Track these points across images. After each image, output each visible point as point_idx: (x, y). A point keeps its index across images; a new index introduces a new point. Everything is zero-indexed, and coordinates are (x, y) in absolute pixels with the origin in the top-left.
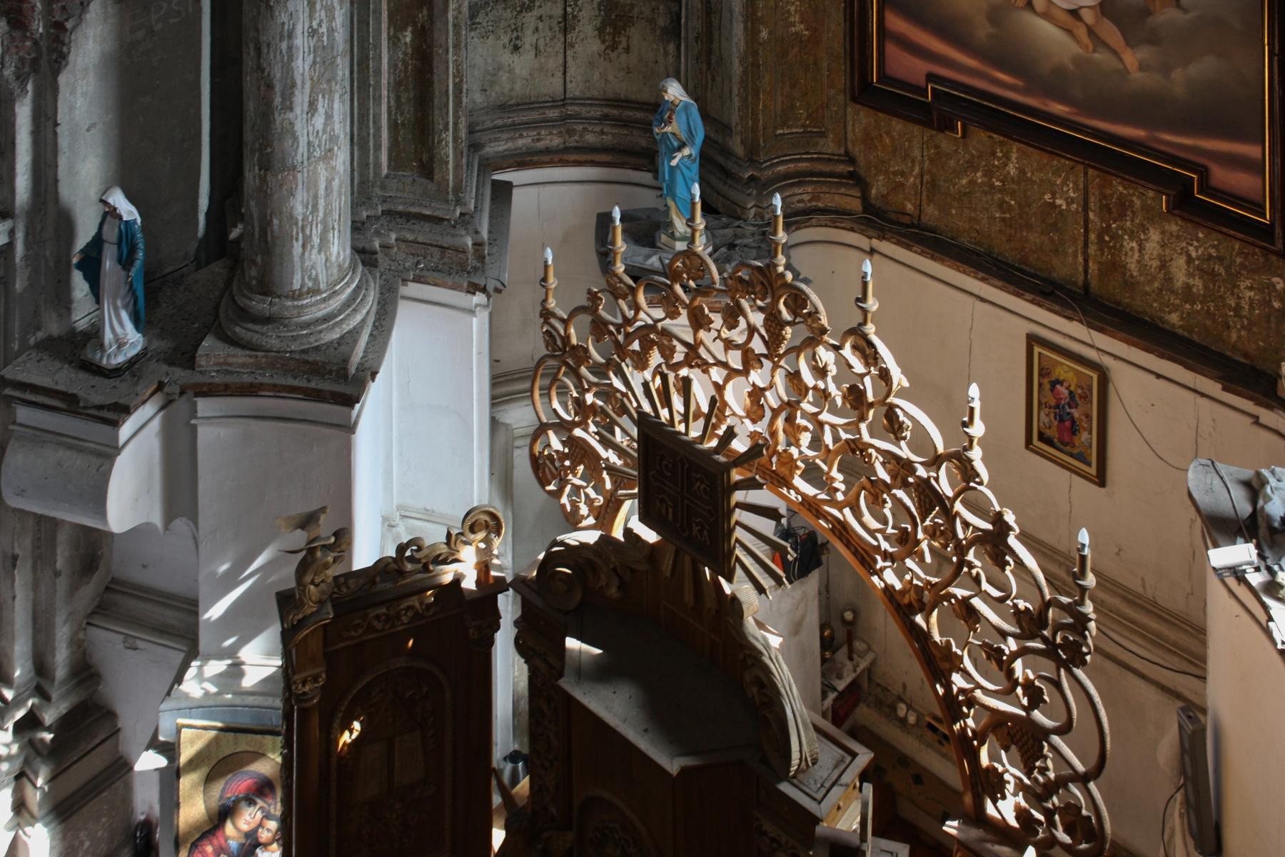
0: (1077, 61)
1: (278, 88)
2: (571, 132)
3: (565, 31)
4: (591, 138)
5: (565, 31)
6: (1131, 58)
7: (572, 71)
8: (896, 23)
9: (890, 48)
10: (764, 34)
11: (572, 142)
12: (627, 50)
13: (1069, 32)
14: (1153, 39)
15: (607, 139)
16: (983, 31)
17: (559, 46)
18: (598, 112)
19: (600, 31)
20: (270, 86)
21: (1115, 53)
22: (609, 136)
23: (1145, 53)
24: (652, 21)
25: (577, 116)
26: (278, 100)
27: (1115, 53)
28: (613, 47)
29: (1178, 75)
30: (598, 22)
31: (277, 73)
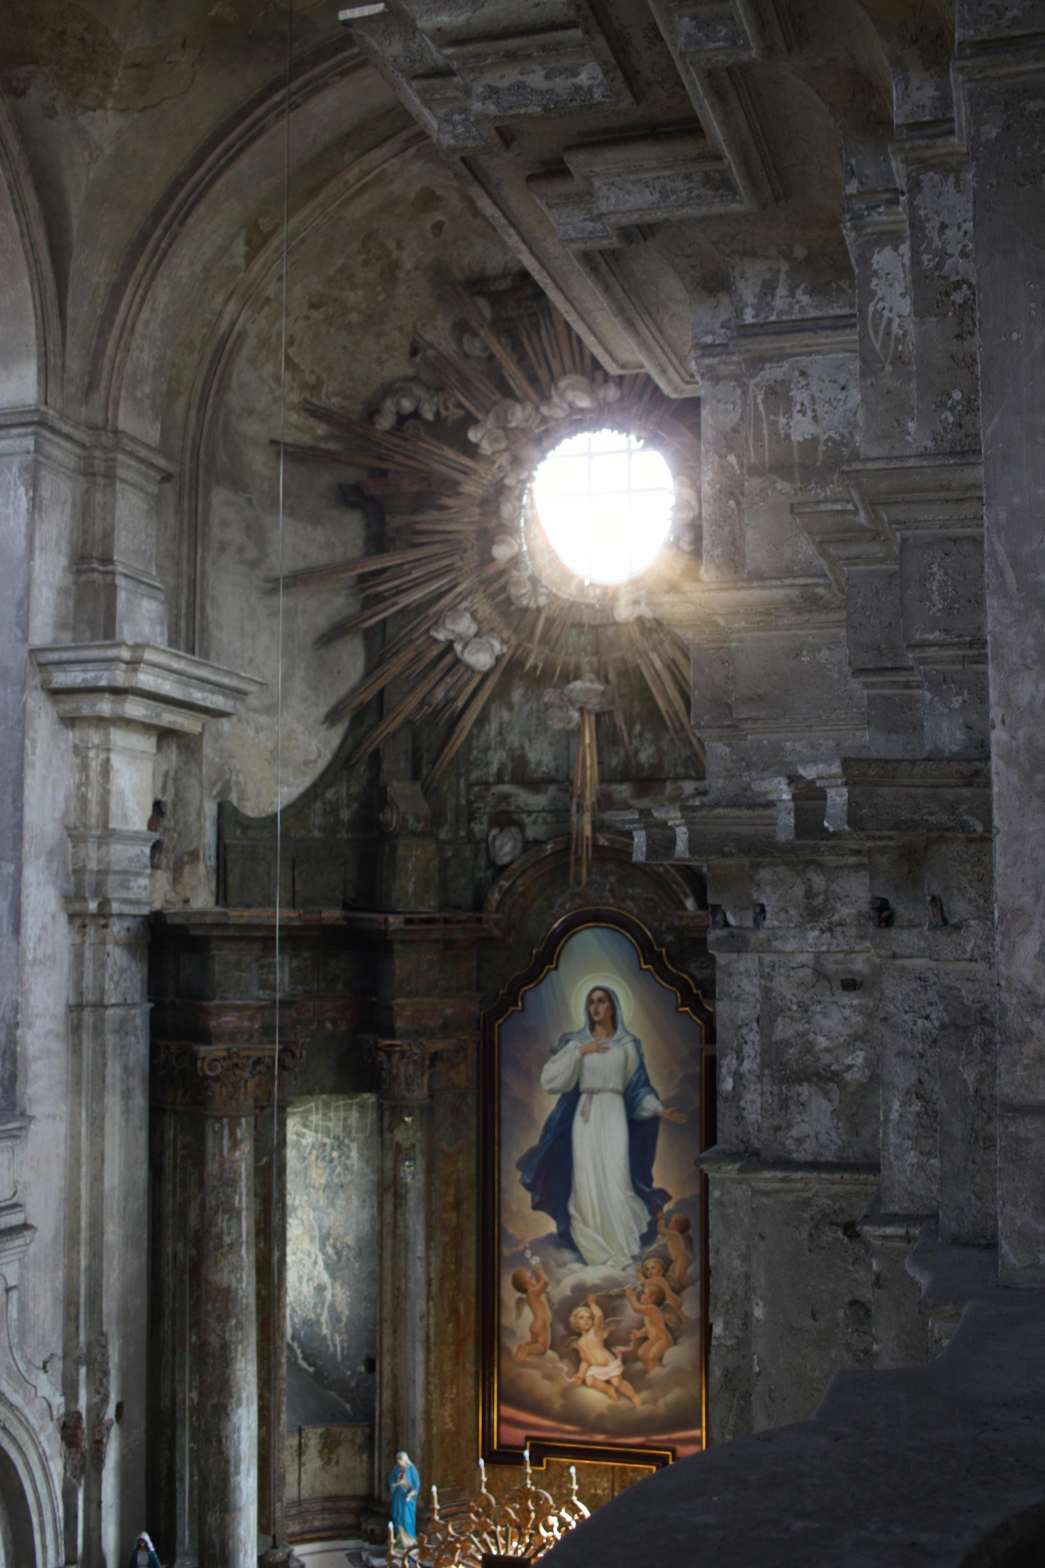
0: (610, 1408)
1: (232, 1462)
2: (305, 1521)
3: (300, 1456)
4: (317, 1524)
5: (300, 1456)
6: (637, 1399)
7: (304, 1481)
8: (508, 1411)
9: (503, 1427)
10: (435, 1430)
11: (306, 1527)
12: (337, 1463)
13: (605, 1392)
14: (649, 1386)
15: (327, 1523)
16: (558, 1403)
17: (296, 1466)
18: (318, 1508)
19: (321, 1452)
20: (227, 1462)
21: (629, 1399)
22: (329, 1520)
23: (645, 1395)
24: (353, 1442)
25: (307, 1511)
26: (232, 1469)
27: (629, 1399)
28: (328, 1463)
29: (661, 1403)
30: (319, 1447)
31: (232, 1453)
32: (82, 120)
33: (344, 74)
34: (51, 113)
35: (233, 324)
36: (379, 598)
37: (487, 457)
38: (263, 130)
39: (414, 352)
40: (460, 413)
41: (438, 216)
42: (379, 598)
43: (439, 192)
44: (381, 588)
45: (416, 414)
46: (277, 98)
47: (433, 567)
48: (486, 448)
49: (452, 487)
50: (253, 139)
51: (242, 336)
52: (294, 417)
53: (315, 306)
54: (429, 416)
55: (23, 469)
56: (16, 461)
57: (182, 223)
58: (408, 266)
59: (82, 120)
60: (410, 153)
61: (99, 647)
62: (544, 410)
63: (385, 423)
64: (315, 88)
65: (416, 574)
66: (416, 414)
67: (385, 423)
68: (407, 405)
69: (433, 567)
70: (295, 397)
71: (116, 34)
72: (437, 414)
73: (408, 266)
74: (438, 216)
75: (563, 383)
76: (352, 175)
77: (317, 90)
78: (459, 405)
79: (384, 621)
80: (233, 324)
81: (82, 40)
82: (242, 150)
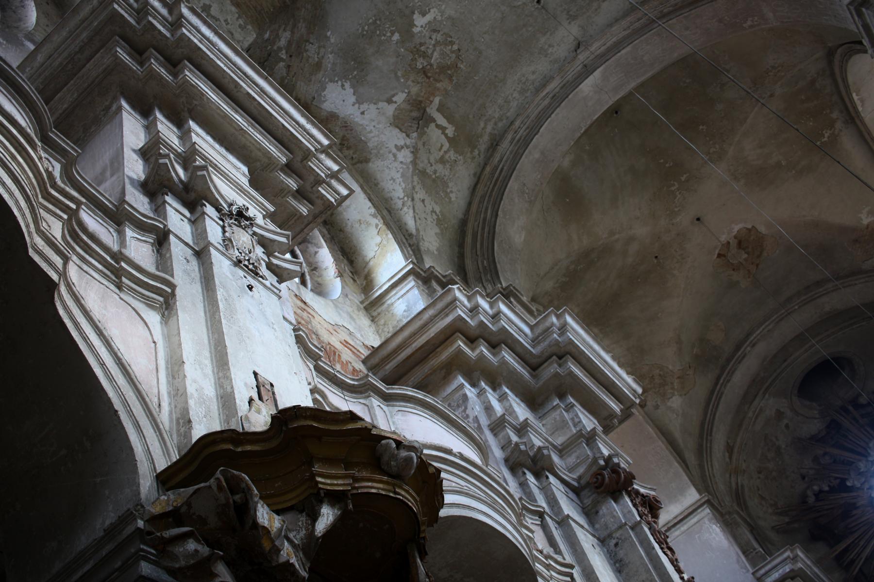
32: (669, 404)
33: (740, 363)
34: (657, 407)
35: (737, 484)
36: (853, 561)
37: (858, 488)
38: (722, 394)
39: (803, 478)
40: (838, 481)
41: (786, 421)
42: (853, 561)
43: (782, 410)
44: (851, 557)
45: (821, 491)
46: (721, 381)
47: (867, 537)
48: (858, 485)
49: (854, 506)
50: (720, 398)
51: (742, 486)
52: (774, 518)
53: (759, 472)
54: (826, 489)
55: (710, 520)
56: (706, 520)
57: (711, 435)
58: (783, 446)
59: (669, 404)
60: (767, 396)
61: (779, 556)
62: (871, 459)
63: (811, 500)
64: (732, 372)
65: (862, 543)
66: (821, 491)
67: (811, 500)
68: (816, 488)
69: (867, 537)
70: (770, 510)
71: (670, 367)
72: (829, 486)
73: (783, 446)
74: (786, 421)
75: (871, 445)
76: (750, 414)
77: (733, 372)
78: (836, 478)
79: (860, 569)
80: (737, 484)
81: (660, 375)
82: (718, 404)
